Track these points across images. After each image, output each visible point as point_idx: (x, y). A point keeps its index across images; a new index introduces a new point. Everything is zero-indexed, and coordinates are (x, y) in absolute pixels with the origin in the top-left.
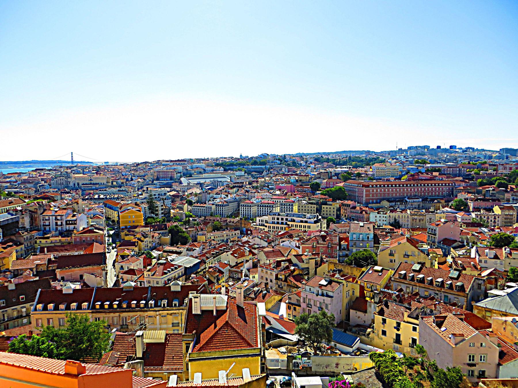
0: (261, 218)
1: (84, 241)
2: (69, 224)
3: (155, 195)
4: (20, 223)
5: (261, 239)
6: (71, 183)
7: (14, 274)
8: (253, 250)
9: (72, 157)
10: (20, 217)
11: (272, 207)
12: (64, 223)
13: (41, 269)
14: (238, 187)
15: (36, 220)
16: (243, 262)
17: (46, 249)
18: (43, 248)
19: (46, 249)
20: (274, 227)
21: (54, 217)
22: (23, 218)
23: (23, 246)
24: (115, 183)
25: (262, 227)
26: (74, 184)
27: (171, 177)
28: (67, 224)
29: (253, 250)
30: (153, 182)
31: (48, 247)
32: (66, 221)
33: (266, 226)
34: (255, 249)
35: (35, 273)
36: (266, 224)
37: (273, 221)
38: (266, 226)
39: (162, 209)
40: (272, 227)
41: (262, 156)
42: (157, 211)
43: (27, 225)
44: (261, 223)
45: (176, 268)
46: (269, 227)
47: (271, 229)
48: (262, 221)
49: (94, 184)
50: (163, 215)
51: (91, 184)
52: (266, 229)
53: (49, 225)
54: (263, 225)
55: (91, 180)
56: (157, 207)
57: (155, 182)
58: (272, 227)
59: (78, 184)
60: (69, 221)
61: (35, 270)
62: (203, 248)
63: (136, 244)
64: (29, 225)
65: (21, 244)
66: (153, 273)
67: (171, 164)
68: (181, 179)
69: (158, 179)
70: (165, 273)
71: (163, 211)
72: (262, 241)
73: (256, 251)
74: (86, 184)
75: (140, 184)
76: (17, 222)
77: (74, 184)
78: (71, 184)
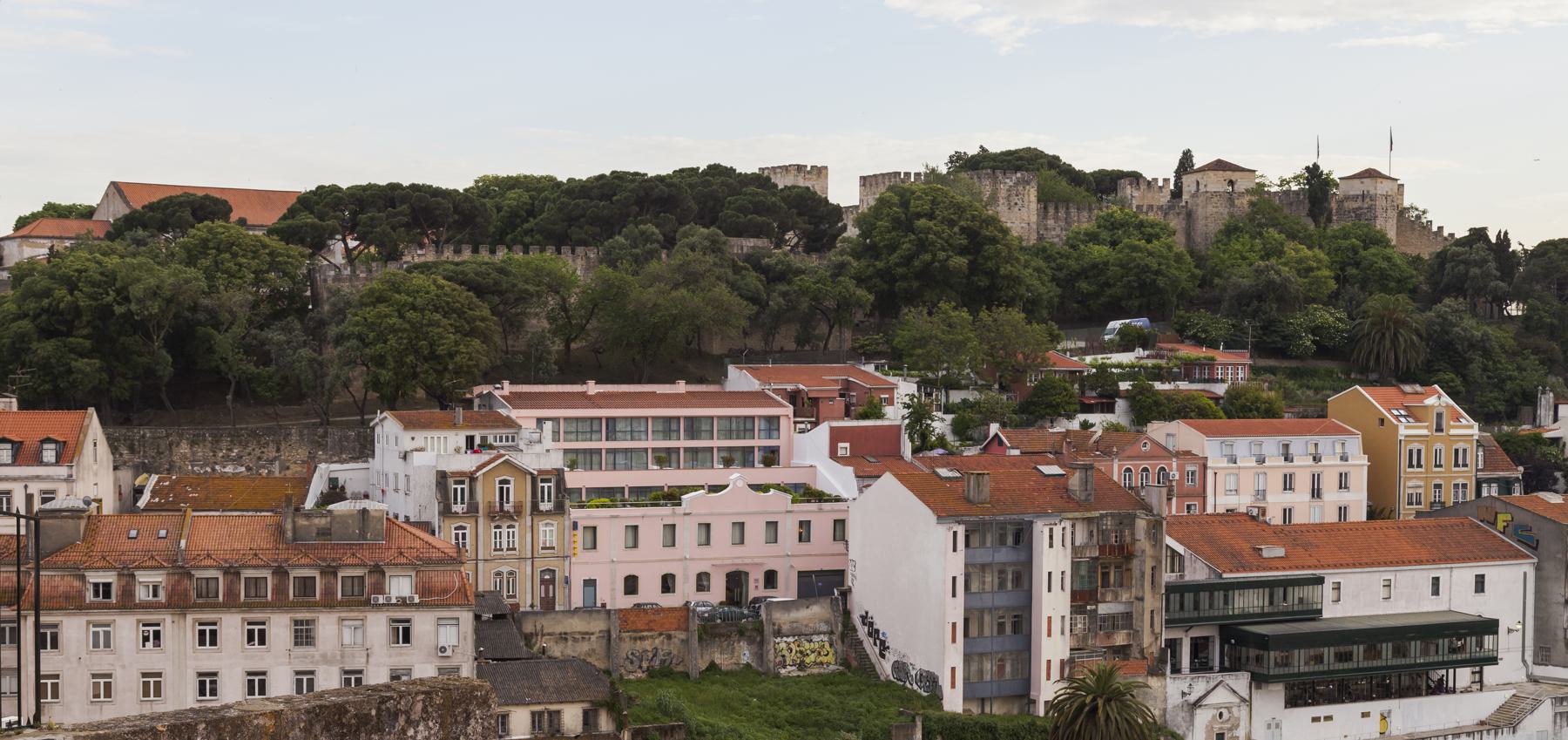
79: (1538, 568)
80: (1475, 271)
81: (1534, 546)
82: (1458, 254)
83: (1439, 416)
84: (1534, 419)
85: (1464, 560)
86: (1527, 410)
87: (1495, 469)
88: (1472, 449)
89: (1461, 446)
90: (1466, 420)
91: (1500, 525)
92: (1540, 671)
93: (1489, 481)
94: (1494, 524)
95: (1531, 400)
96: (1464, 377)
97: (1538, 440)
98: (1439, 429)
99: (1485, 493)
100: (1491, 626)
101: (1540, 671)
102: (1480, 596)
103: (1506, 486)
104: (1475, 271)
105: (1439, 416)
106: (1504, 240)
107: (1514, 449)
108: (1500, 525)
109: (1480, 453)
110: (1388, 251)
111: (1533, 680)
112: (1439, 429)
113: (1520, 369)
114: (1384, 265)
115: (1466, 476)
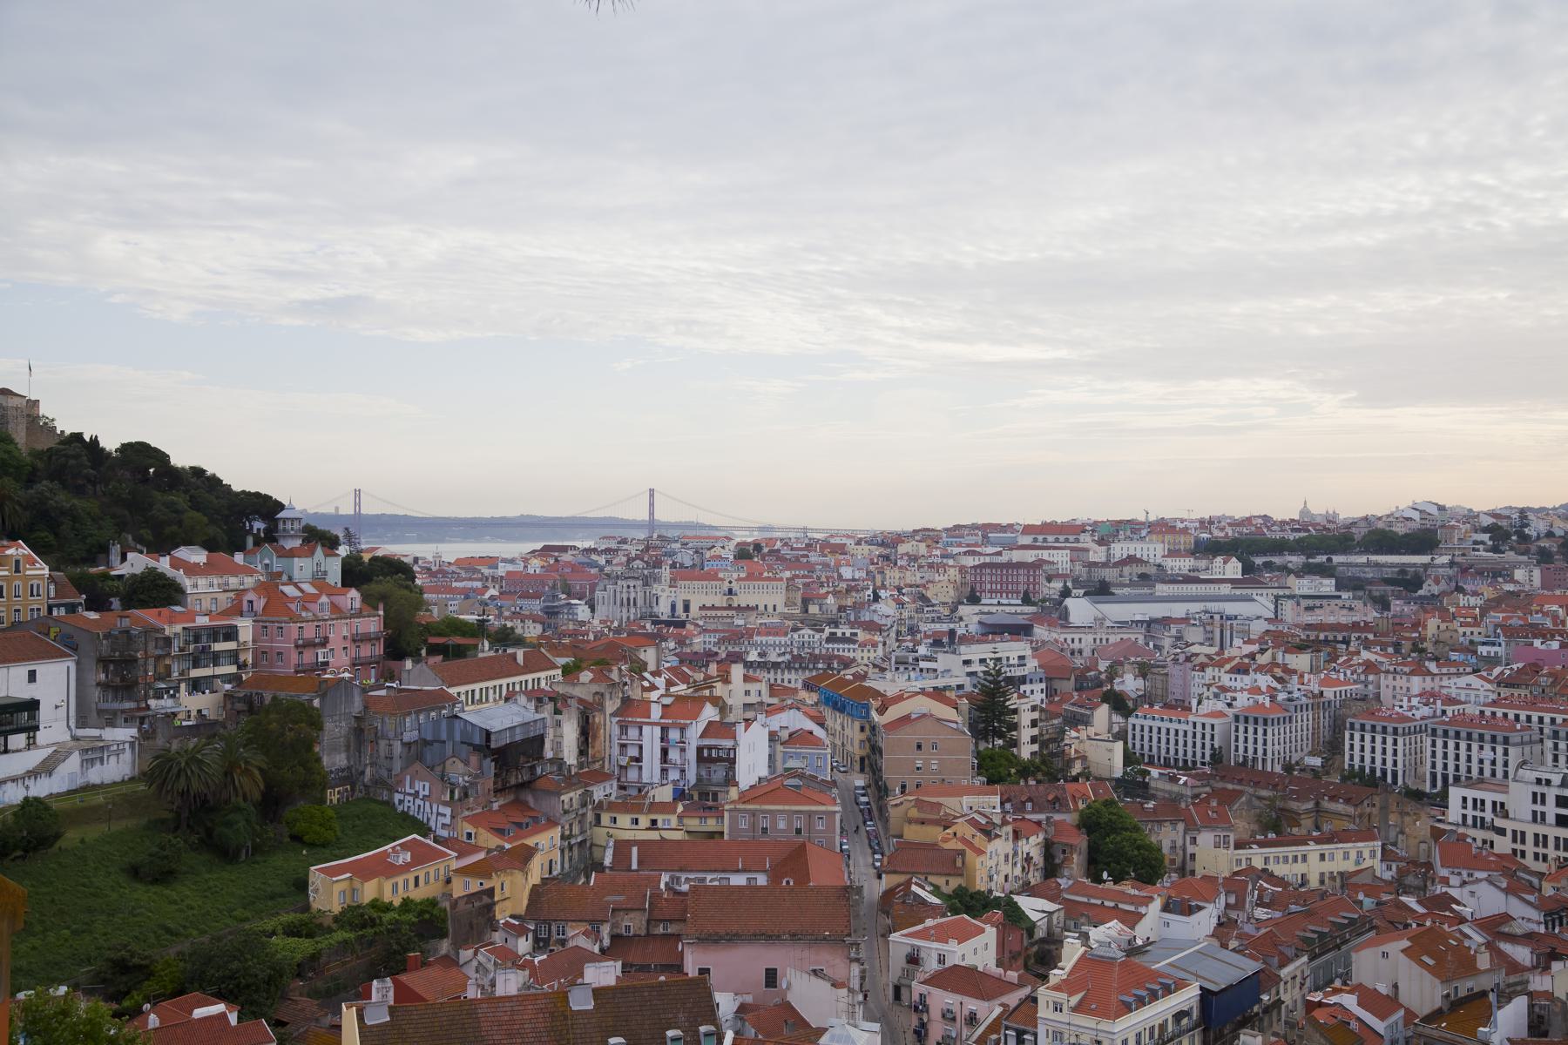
0: (1471, 794)
1: (765, 830)
2: (711, 760)
3: (982, 661)
4: (548, 745)
5: (1507, 891)
6: (661, 601)
7: (536, 940)
8: (1506, 947)
9: (652, 505)
10: (549, 722)
11: (1506, 741)
12: (692, 754)
13: (628, 928)
14: (1326, 641)
15: (595, 737)
16: (1484, 994)
17: (635, 850)
18: (629, 844)
19: (635, 850)
20: (1541, 840)
21: (657, 731)
22: (558, 724)
23: (556, 833)
24: (814, 609)
25: (1480, 834)
26: (673, 607)
27: (1026, 593)
28: (701, 759)
29: (1506, 947)
30: (954, 610)
31: (641, 844)
32: (700, 750)
33: (1502, 832)
34: (1512, 938)
35: (607, 942)
36: (1499, 823)
37: (1539, 808)
38: (1502, 832)
39: (1034, 723)
40: (1530, 839)
41: (1416, 516)
42: (1015, 727)
43: (570, 756)
44: (1470, 812)
45: (1168, 991)
46: (1518, 837)
47: (1530, 848)
48: (1479, 804)
49: (739, 608)
50: (1036, 747)
51: (730, 607)
52: (1504, 845)
53: (639, 760)
54: (1480, 823)
55: (730, 592)
56: (1015, 711)
57: (964, 610)
58: (1530, 839)
59: (687, 608)
60: (710, 748)
61: (605, 930)
62: (1227, 906)
63: (959, 864)
64: (575, 751)
65: (552, 823)
66: (1075, 1000)
67: (1027, 540)
68: (1069, 602)
69: (974, 599)
70: (1127, 1008)
71: (1035, 731)
72: (1513, 901)
73: (1522, 954)
74: (713, 608)
75: (906, 614)
76: (540, 740)
77: (673, 607)
78: (663, 610)
79: (78, 663)
80: (72, 462)
81: (75, 649)
82: (58, 451)
83: (17, 562)
84: (108, 564)
85: (19, 660)
86: (102, 556)
87: (64, 597)
88: (43, 584)
89: (35, 582)
90: (40, 563)
91: (52, 635)
92: (81, 732)
93: (59, 606)
94: (47, 634)
95: (105, 550)
96: (56, 535)
97: (105, 576)
98: (17, 570)
99: (55, 613)
100: (33, 706)
101: (81, 732)
102: (32, 685)
103: (72, 608)
104: (72, 462)
105: (17, 562)
106: (95, 442)
107: (80, 584)
108: (52, 635)
109: (52, 587)
110: (11, 447)
111: (75, 738)
112: (17, 570)
113: (100, 528)
114: (6, 456)
115: (40, 603)
